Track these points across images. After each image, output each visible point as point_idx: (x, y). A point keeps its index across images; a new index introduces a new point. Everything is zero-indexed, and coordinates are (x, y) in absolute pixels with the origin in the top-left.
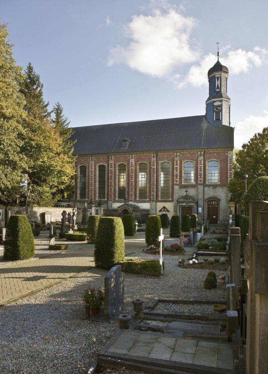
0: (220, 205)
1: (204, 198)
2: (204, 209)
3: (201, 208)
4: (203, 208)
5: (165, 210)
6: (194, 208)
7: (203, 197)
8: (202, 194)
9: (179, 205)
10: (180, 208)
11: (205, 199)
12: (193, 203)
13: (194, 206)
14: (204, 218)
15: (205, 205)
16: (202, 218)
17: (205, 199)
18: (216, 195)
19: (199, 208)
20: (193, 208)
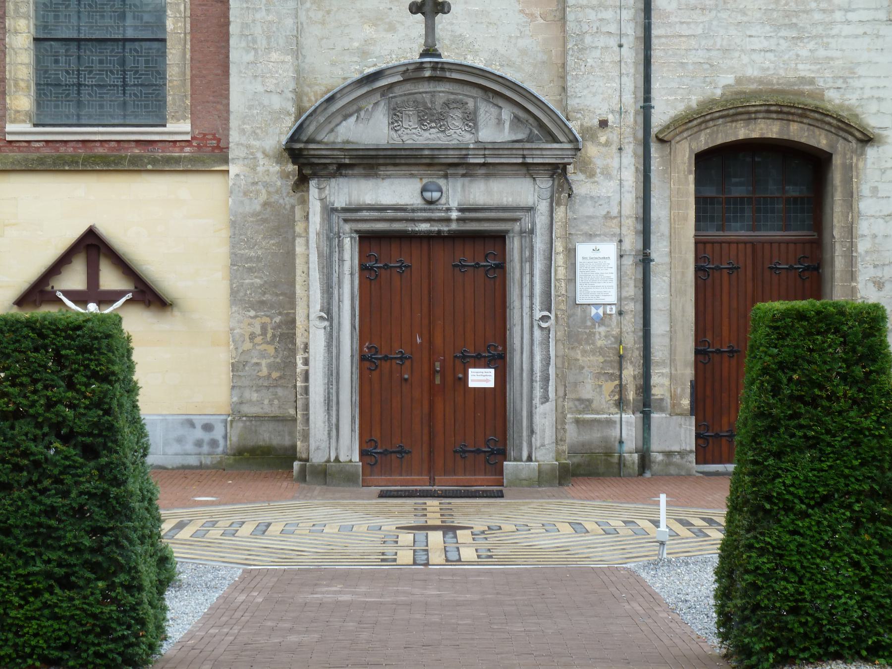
0: (866, 206)
1: (646, 109)
2: (645, 261)
3: (609, 250)
4: (632, 242)
5: (110, 280)
6: (539, 244)
7: (631, 100)
8: (630, 54)
9: (329, 211)
10: (332, 238)
11: (661, 117)
12: (528, 169)
13: (541, 220)
14: (645, 388)
15: (659, 212)
16: (621, 388)
17: (661, 117)
18: (805, 70)
19: (584, 250)
20: (514, 246)
